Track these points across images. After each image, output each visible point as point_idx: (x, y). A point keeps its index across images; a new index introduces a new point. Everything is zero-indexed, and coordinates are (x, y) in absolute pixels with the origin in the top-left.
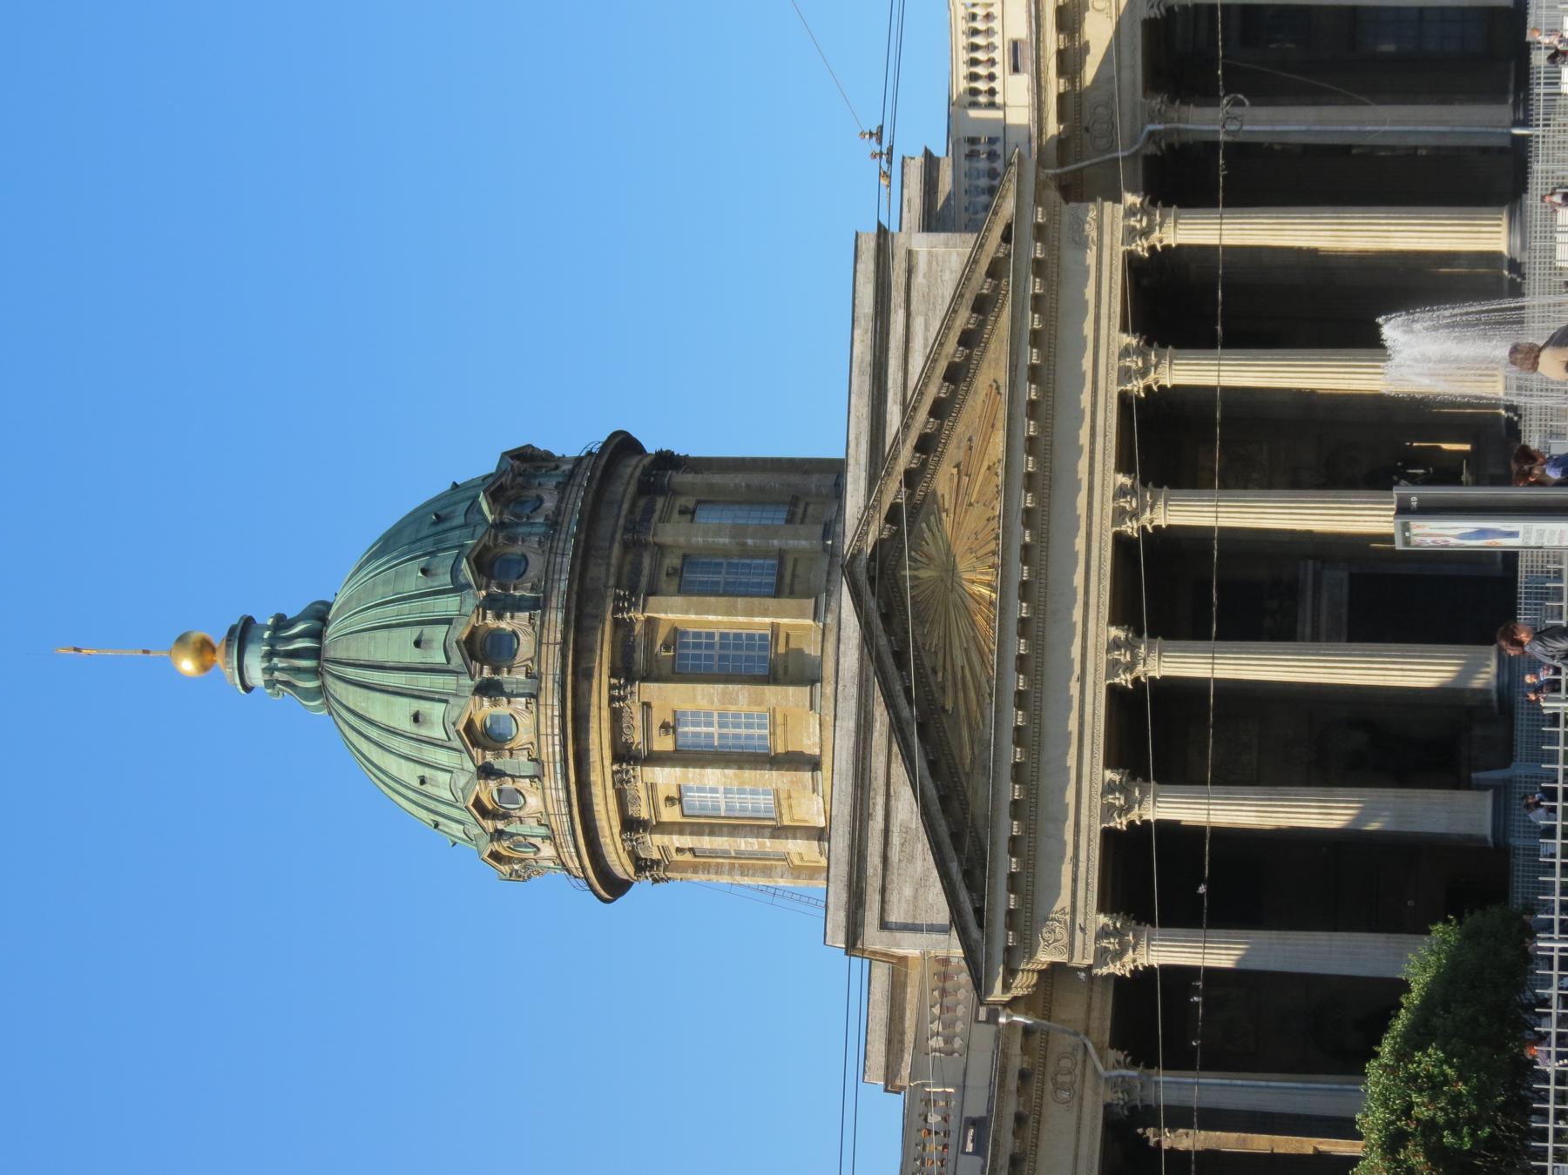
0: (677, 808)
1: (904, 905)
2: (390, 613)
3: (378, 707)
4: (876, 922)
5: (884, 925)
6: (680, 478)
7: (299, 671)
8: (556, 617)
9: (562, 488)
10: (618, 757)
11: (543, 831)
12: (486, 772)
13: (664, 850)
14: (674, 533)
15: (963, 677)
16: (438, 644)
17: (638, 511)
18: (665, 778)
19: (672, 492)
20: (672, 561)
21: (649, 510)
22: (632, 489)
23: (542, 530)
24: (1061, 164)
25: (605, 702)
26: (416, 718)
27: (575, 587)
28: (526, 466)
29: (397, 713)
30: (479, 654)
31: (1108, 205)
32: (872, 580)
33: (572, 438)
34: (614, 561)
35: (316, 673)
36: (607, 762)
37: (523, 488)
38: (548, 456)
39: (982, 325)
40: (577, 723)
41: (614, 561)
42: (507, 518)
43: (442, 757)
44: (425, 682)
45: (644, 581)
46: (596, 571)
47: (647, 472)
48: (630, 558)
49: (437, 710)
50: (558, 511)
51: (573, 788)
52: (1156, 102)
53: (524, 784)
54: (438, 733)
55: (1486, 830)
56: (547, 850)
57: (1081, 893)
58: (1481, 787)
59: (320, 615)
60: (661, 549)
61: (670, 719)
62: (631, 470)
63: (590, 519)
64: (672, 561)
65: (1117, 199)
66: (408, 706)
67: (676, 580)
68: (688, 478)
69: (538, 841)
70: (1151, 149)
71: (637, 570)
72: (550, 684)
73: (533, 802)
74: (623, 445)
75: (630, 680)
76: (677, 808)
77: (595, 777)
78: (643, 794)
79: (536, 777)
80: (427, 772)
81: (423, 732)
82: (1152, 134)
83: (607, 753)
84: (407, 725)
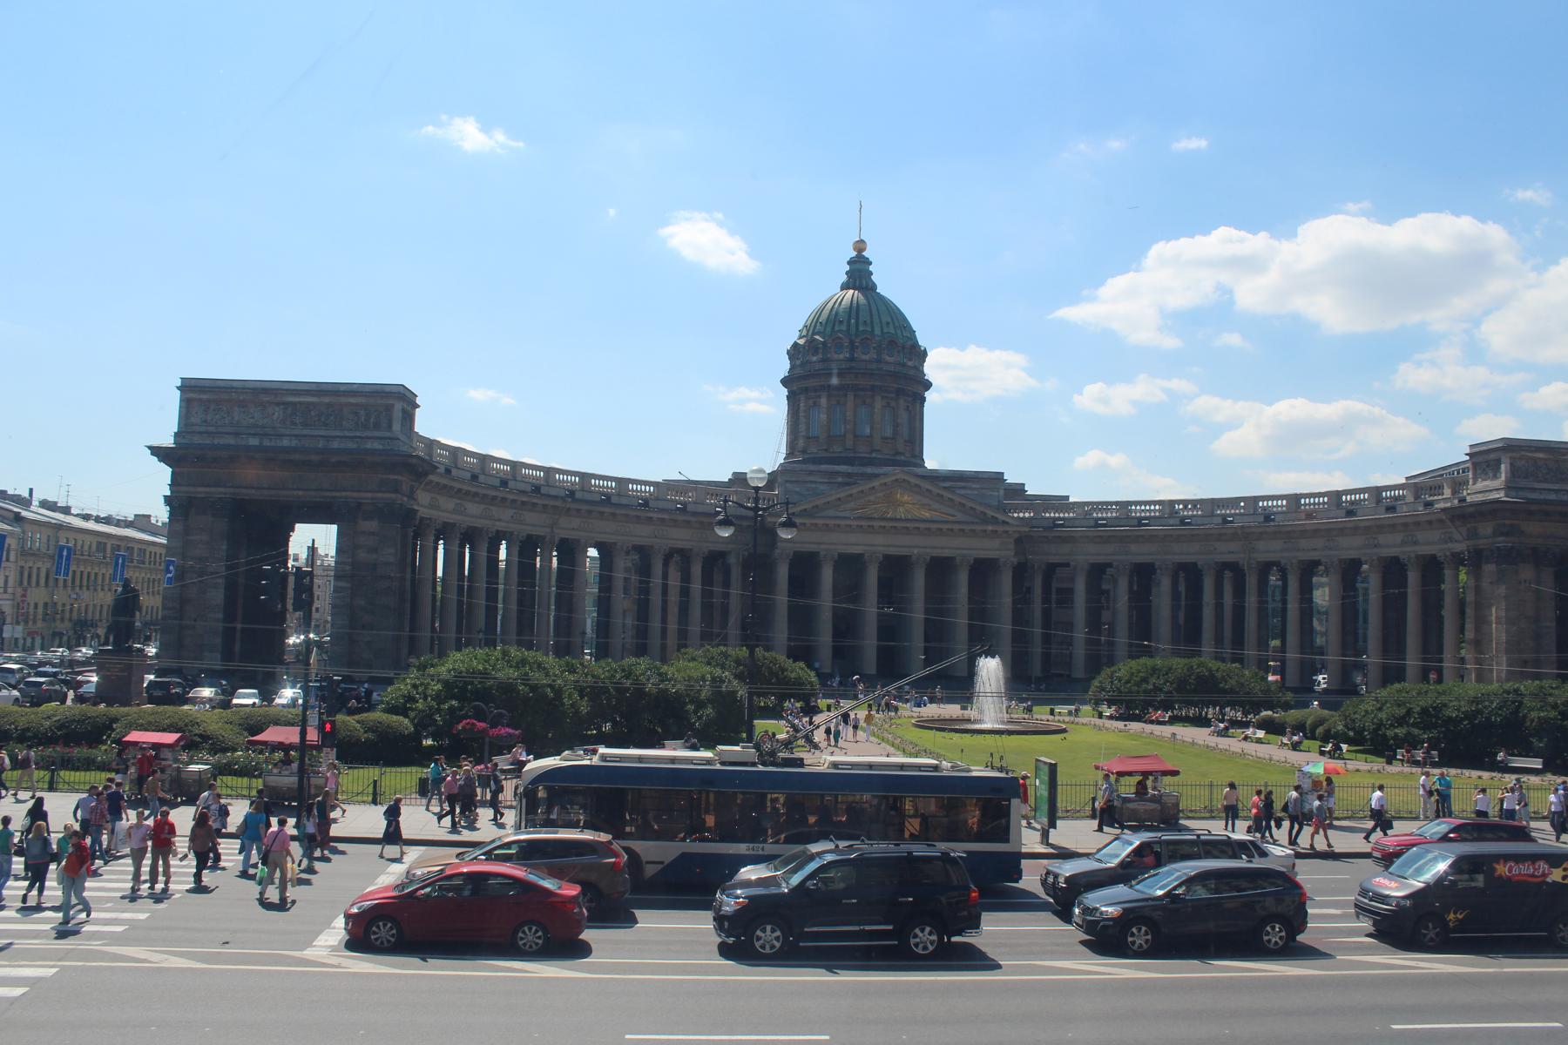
8: (874, 366)
18: (823, 401)
33: (930, 369)
49: (844, 328)
59: (874, 287)
64: (893, 404)
74: (928, 385)
79: (823, 361)
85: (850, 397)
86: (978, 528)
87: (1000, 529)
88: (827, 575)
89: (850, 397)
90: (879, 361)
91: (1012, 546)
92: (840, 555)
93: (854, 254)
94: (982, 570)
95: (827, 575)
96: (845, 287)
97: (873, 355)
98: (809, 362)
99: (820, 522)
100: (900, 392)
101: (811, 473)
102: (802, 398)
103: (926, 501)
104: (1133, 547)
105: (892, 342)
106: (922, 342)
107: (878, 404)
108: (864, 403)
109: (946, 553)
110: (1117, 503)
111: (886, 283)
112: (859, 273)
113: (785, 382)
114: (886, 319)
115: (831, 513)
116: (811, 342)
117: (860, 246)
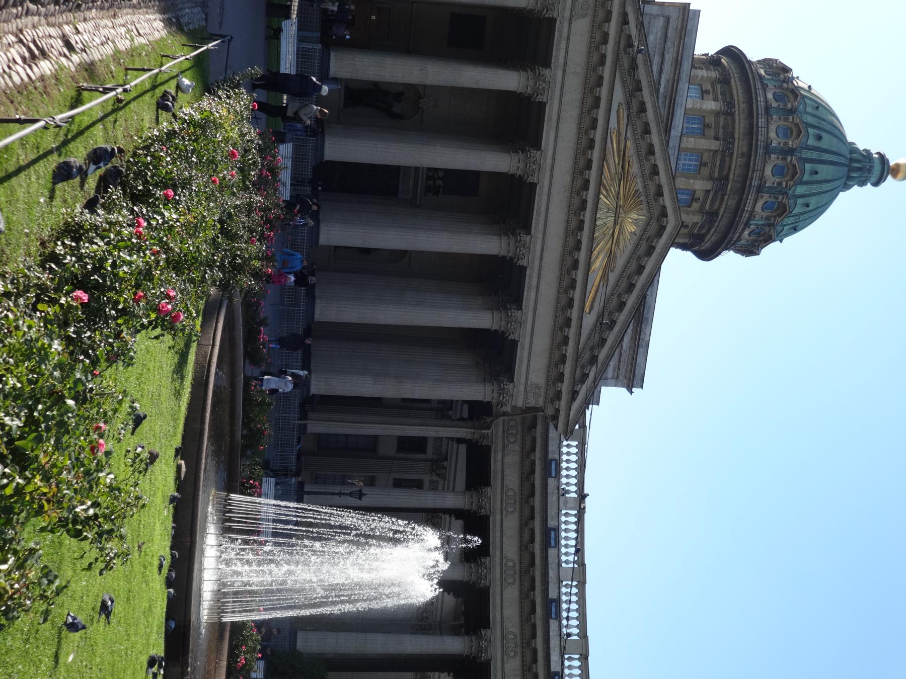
0: (704, 89)
1: (655, 31)
2: (825, 187)
3: (834, 145)
4: (671, 21)
5: (668, 19)
6: (686, 241)
7: (858, 161)
8: (755, 182)
9: (739, 239)
10: (733, 115)
11: (765, 82)
12: (792, 111)
13: (708, 69)
14: (692, 218)
15: (619, 158)
16: (807, 172)
17: (706, 227)
18: (711, 105)
19: (691, 235)
20: (696, 206)
21: (702, 227)
22: (708, 237)
23: (752, 222)
24: (535, 417)
25: (737, 141)
26: (819, 138)
27: (745, 197)
28: (750, 250)
29: (827, 142)
30: (791, 167)
31: (520, 403)
32: (664, 214)
33: (729, 258)
34: (724, 207)
35: (852, 160)
36: (737, 112)
37: (756, 241)
38: (737, 251)
39: (592, 349)
40: (751, 132)
41: (724, 207)
42: (767, 229)
43: (810, 120)
44: (814, 155)
45: (710, 197)
46: (732, 203)
47: (699, 244)
48: (715, 207)
49: (811, 142)
50: (744, 230)
51: (754, 101)
52: (485, 443)
53: (775, 104)
54: (811, 131)
55: (332, 55)
56: (762, 72)
57: (565, 30)
58: (335, 80)
59: (846, 187)
60: (701, 211)
61: (707, 131)
62: (706, 245)
63: (731, 226)
64: (696, 206)
65: (514, 407)
66: (824, 144)
67: (696, 196)
68: (681, 241)
69: (767, 77)
70: (489, 420)
71: (713, 201)
72: (761, 151)
73: (770, 96)
75: (724, 151)
76: (704, 89)
77: (743, 106)
78: (720, 96)
79: (768, 108)
80: (815, 112)
81: (817, 131)
82: (488, 428)
83: (737, 117)
84: (824, 135)
85: (715, 145)
86: (570, 350)
87: (565, 387)
88: (508, 80)
89: (715, 145)
90: (760, 189)
91: (532, 402)
92: (542, 106)
93: (892, 163)
94: (494, 353)
95: (508, 80)
96: (853, 149)
97: (771, 179)
98: (765, 88)
99: (607, 73)
100: (712, 216)
101: (678, 63)
102: (714, 74)
103: (620, 262)
104: (512, 593)
105: (783, 210)
106: (771, 250)
107: (700, 185)
108: (703, 164)
109: (529, 296)
110: (582, 564)
111: (852, 202)
112: (869, 169)
113: (732, 53)
114: (813, 201)
115: (619, 96)
116: (795, 92)
117: (895, 171)
